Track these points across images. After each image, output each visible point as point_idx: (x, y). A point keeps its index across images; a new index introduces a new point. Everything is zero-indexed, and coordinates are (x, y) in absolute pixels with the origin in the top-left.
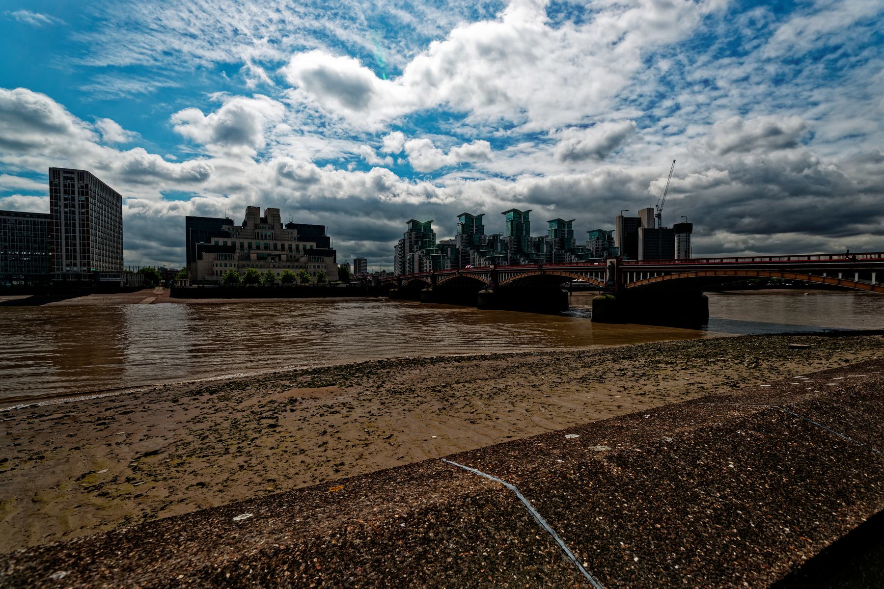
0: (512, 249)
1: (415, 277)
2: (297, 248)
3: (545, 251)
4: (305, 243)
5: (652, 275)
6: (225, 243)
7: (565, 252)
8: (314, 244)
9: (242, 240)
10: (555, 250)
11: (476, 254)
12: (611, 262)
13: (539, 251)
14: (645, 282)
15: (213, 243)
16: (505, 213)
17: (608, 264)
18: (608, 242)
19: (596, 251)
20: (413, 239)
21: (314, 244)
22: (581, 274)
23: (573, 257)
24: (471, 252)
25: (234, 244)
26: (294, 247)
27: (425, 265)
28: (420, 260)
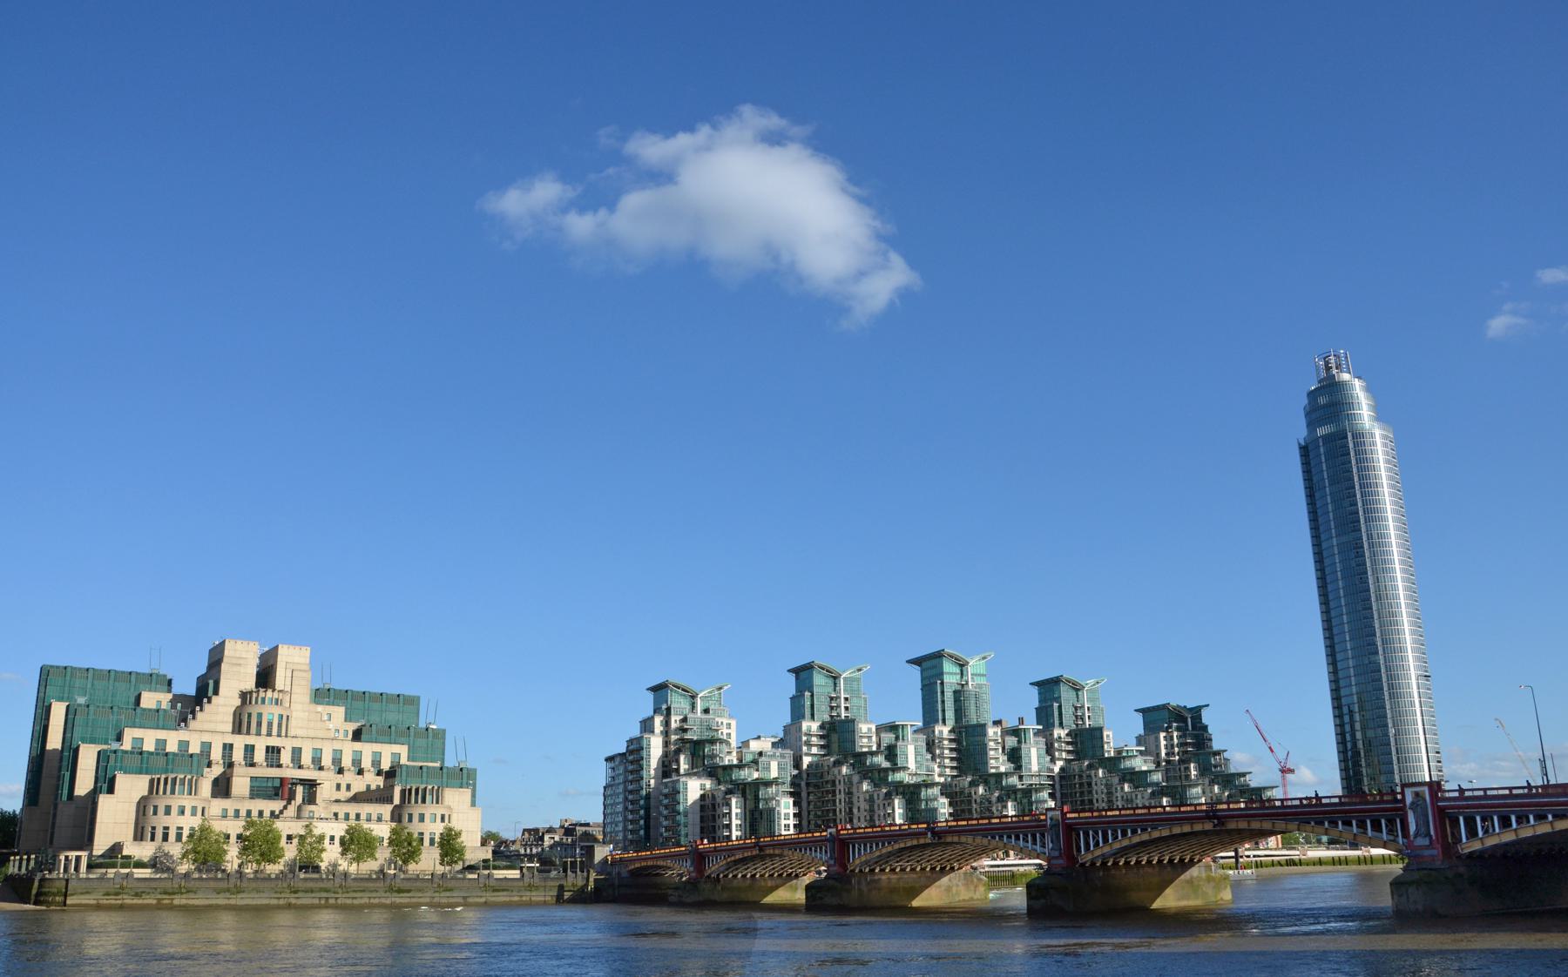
2: (357, 762)
3: (1035, 768)
4: (377, 747)
5: (1505, 823)
6: (161, 743)
8: (403, 750)
9: (206, 738)
12: (1417, 794)
13: (1019, 767)
14: (1508, 837)
15: (127, 745)
17: (1409, 799)
18: (1195, 737)
21: (403, 750)
22: (1334, 823)
23: (1116, 780)
25: (207, 748)
26: (347, 762)
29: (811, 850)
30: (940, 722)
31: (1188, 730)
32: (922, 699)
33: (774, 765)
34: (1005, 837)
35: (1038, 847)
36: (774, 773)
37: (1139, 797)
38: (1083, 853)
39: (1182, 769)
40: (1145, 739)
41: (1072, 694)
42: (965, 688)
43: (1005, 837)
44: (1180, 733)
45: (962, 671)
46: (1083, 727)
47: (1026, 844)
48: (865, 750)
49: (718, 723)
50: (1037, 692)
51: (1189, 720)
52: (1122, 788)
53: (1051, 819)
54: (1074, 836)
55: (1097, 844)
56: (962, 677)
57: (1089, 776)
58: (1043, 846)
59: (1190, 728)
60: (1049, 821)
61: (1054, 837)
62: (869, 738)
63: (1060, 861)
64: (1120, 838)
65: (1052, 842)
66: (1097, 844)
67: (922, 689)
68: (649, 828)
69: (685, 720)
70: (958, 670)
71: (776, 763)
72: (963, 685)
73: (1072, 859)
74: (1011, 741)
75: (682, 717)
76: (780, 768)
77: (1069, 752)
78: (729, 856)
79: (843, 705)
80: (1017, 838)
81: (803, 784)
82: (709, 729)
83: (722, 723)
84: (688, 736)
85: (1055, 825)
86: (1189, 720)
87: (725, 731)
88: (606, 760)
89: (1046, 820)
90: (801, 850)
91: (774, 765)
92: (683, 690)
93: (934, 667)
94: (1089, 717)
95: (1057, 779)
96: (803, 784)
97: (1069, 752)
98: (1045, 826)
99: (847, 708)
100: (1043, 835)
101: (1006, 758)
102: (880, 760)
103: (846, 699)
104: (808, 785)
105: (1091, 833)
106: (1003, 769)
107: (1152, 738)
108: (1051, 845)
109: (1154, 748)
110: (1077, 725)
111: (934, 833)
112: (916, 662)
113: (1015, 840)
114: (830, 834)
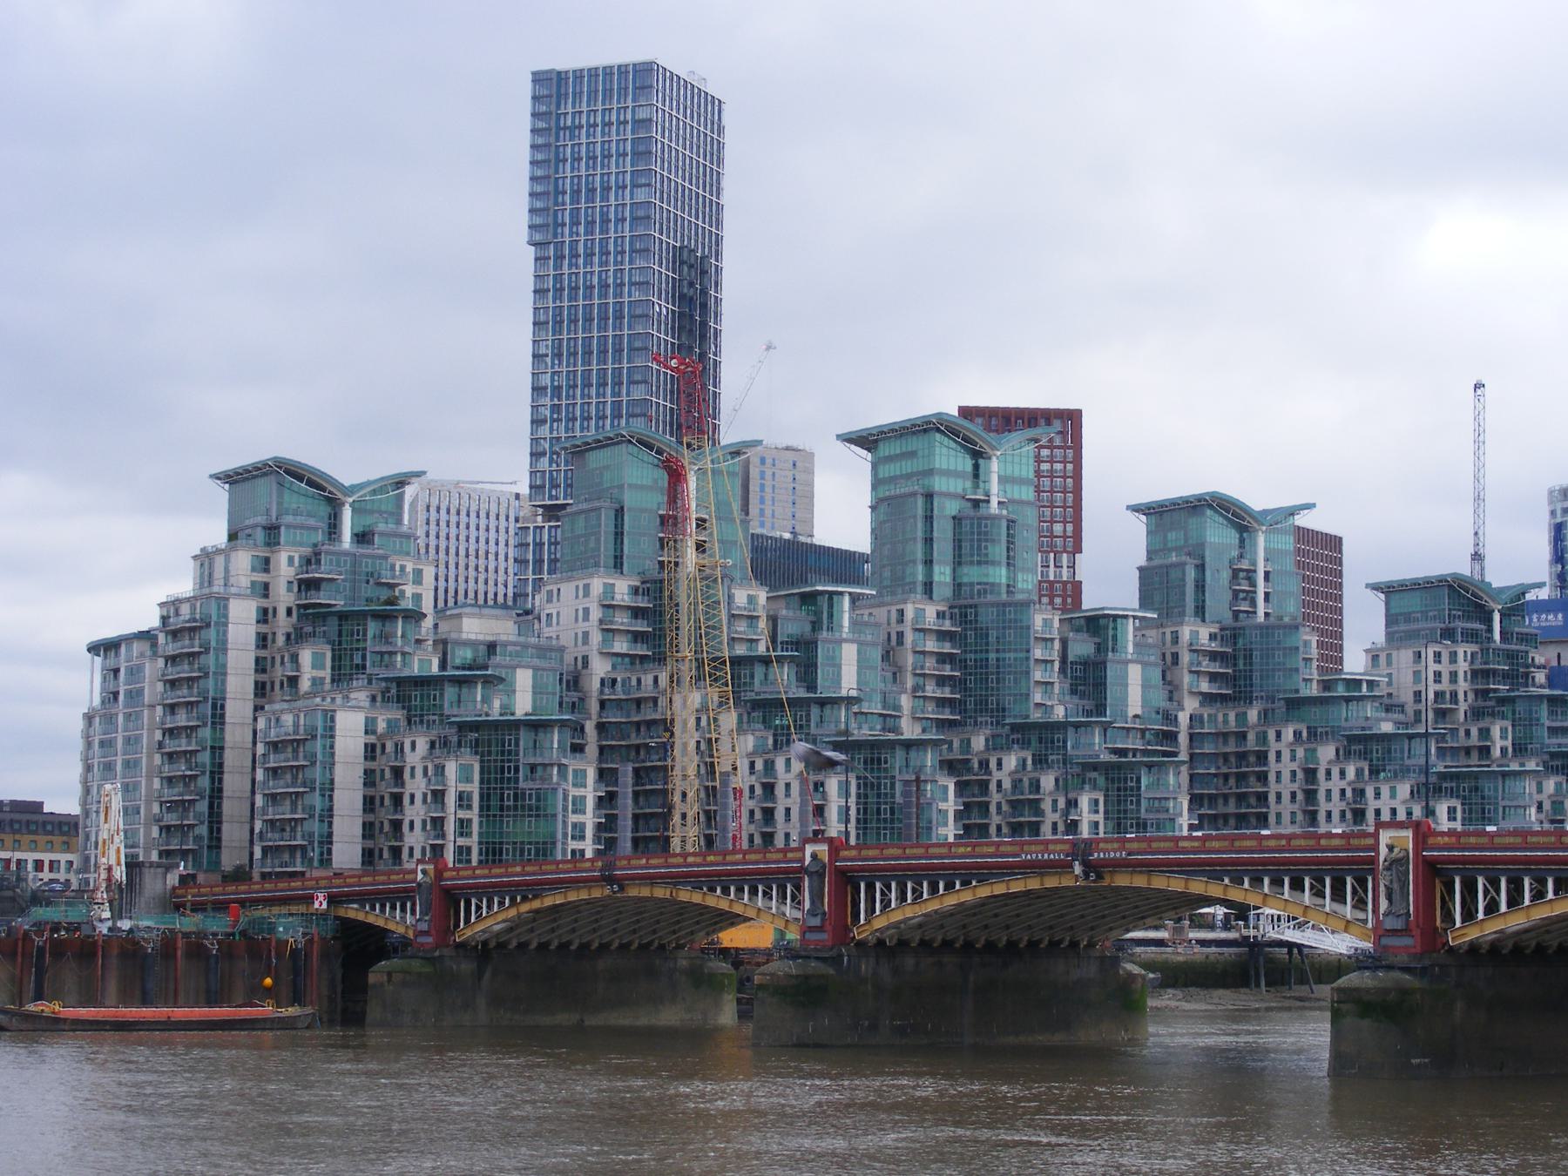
0: (931, 690)
1: (621, 883)
3: (1135, 705)
7: (1265, 715)
10: (1191, 705)
13: (1100, 709)
16: (866, 440)
19: (1441, 714)
20: (284, 597)
23: (1326, 752)
24: (687, 703)
27: (416, 785)
28: (371, 751)
29: (754, 892)
30: (920, 588)
31: (1490, 639)
32: (873, 531)
33: (523, 680)
34: (1266, 881)
35: (1348, 910)
36: (523, 705)
37: (1385, 791)
38: (1458, 924)
39: (1474, 732)
40: (1389, 656)
41: (1232, 536)
42: (983, 511)
43: (1266, 881)
44: (1474, 648)
45: (976, 467)
46: (1250, 622)
47: (1319, 901)
48: (741, 650)
49: (393, 568)
50: (1143, 529)
51: (1497, 617)
52: (1342, 773)
53: (1391, 848)
54: (1439, 887)
55: (1492, 908)
56: (976, 486)
57: (1263, 738)
58: (1360, 904)
59: (1497, 636)
60: (1383, 851)
61: (1396, 886)
62: (752, 619)
63: (1407, 941)
64: (1550, 895)
65: (1389, 898)
66: (1492, 908)
67: (873, 508)
68: (220, 822)
69: (311, 561)
70: (967, 464)
71: (529, 673)
72: (976, 504)
73: (1432, 937)
74: (1082, 647)
75: (307, 550)
76: (537, 690)
77: (1213, 677)
78: (525, 899)
80: (1297, 885)
81: (590, 727)
82: (372, 577)
83: (403, 568)
84: (322, 598)
85: (1397, 864)
86: (1497, 617)
87: (409, 590)
88: (89, 650)
89: (1376, 848)
90: (726, 891)
91: (523, 680)
92: (311, 483)
93: (912, 455)
94: (1267, 595)
95: (1183, 739)
96: (590, 727)
97: (1213, 677)
98: (1373, 861)
99: (700, 547)
100: (1361, 882)
101: (1067, 686)
102: (784, 681)
104: (601, 727)
105: (1349, 880)
106: (1059, 713)
107: (1404, 657)
108: (1384, 905)
109: (1410, 678)
110: (1236, 614)
111: (1088, 866)
112: (866, 440)
113: (1292, 887)
114: (814, 856)
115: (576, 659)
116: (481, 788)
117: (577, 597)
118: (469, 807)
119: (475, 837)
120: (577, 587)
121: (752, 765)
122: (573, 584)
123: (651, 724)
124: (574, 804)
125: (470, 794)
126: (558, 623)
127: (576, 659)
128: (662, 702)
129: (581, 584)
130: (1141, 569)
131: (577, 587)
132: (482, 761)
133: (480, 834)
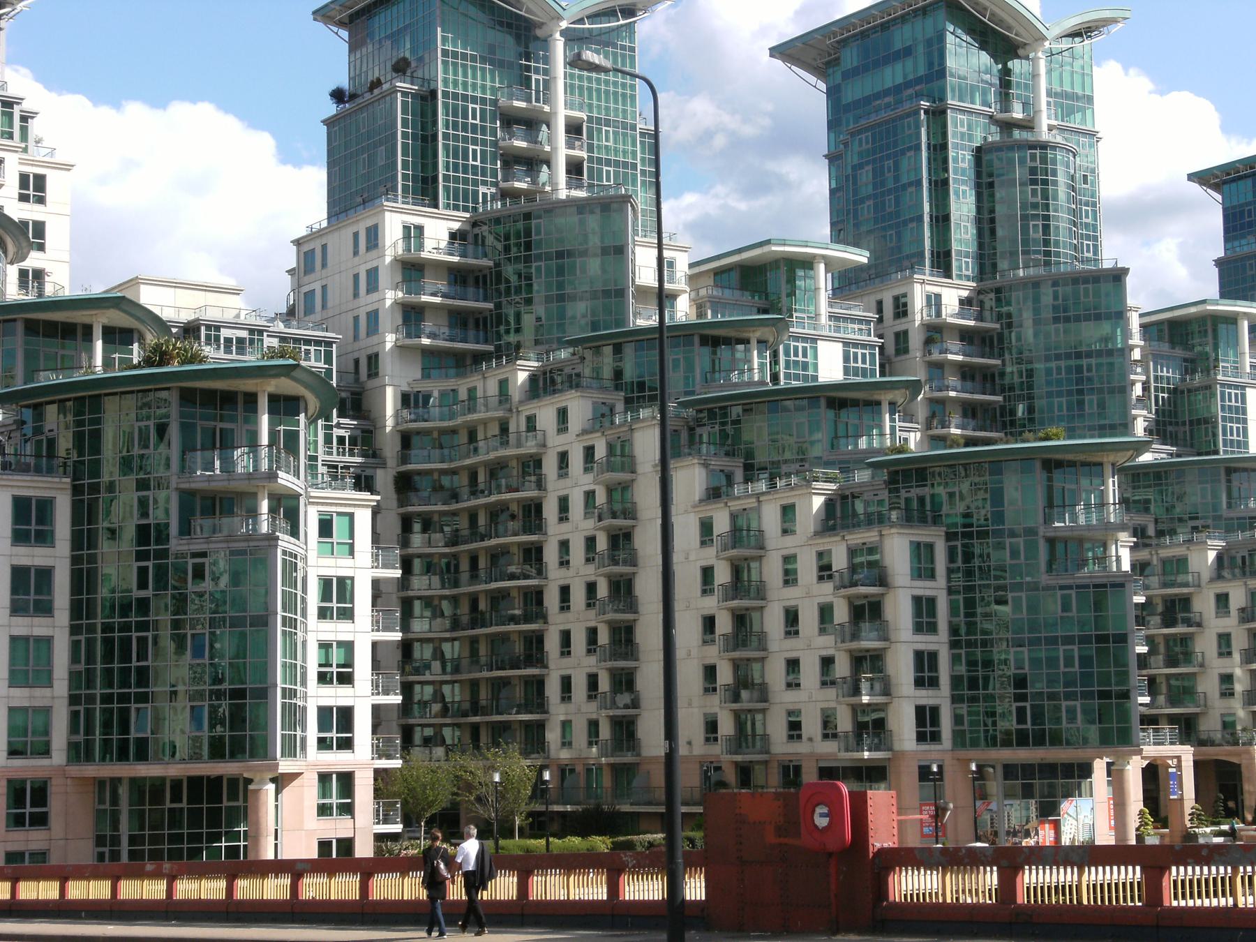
11: (647, 444)
79: (562, 154)
103: (574, 129)
115: (357, 362)
116: (75, 560)
117: (356, 253)
118: (44, 609)
119: (61, 686)
120: (356, 235)
121: (706, 528)
122: (347, 234)
123: (496, 469)
124: (326, 595)
125: (45, 575)
126: (324, 306)
127: (357, 362)
128: (517, 424)
129: (362, 228)
130: (1219, 263)
131: (356, 235)
132: (76, 490)
133: (74, 677)
